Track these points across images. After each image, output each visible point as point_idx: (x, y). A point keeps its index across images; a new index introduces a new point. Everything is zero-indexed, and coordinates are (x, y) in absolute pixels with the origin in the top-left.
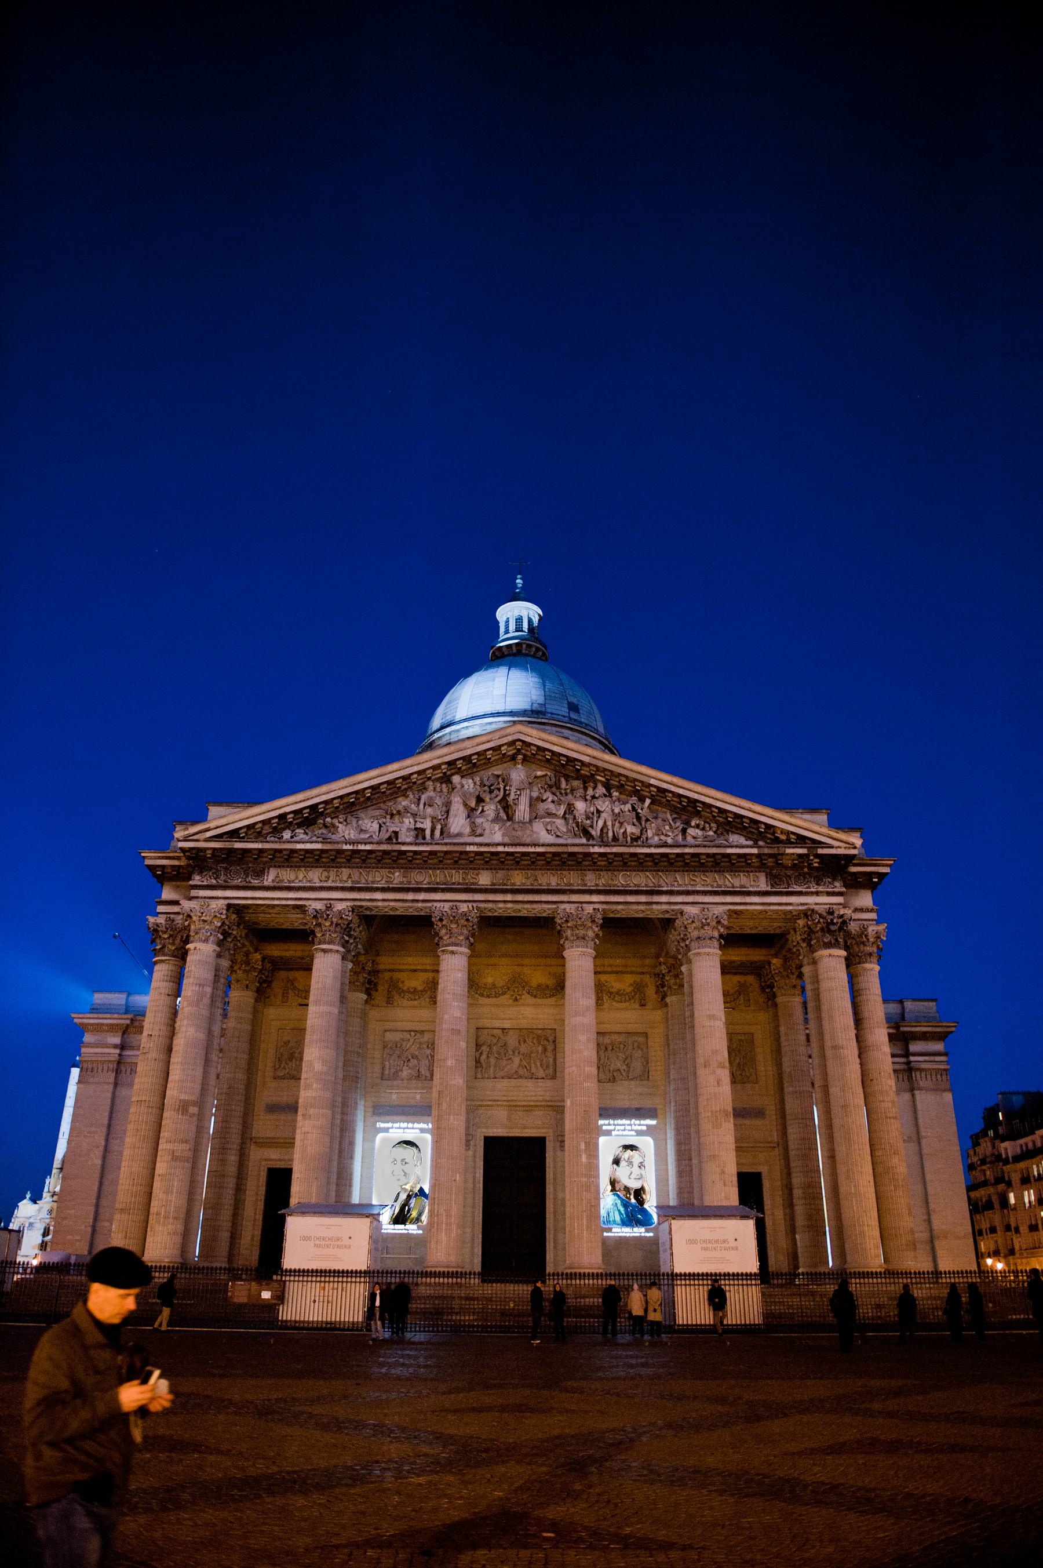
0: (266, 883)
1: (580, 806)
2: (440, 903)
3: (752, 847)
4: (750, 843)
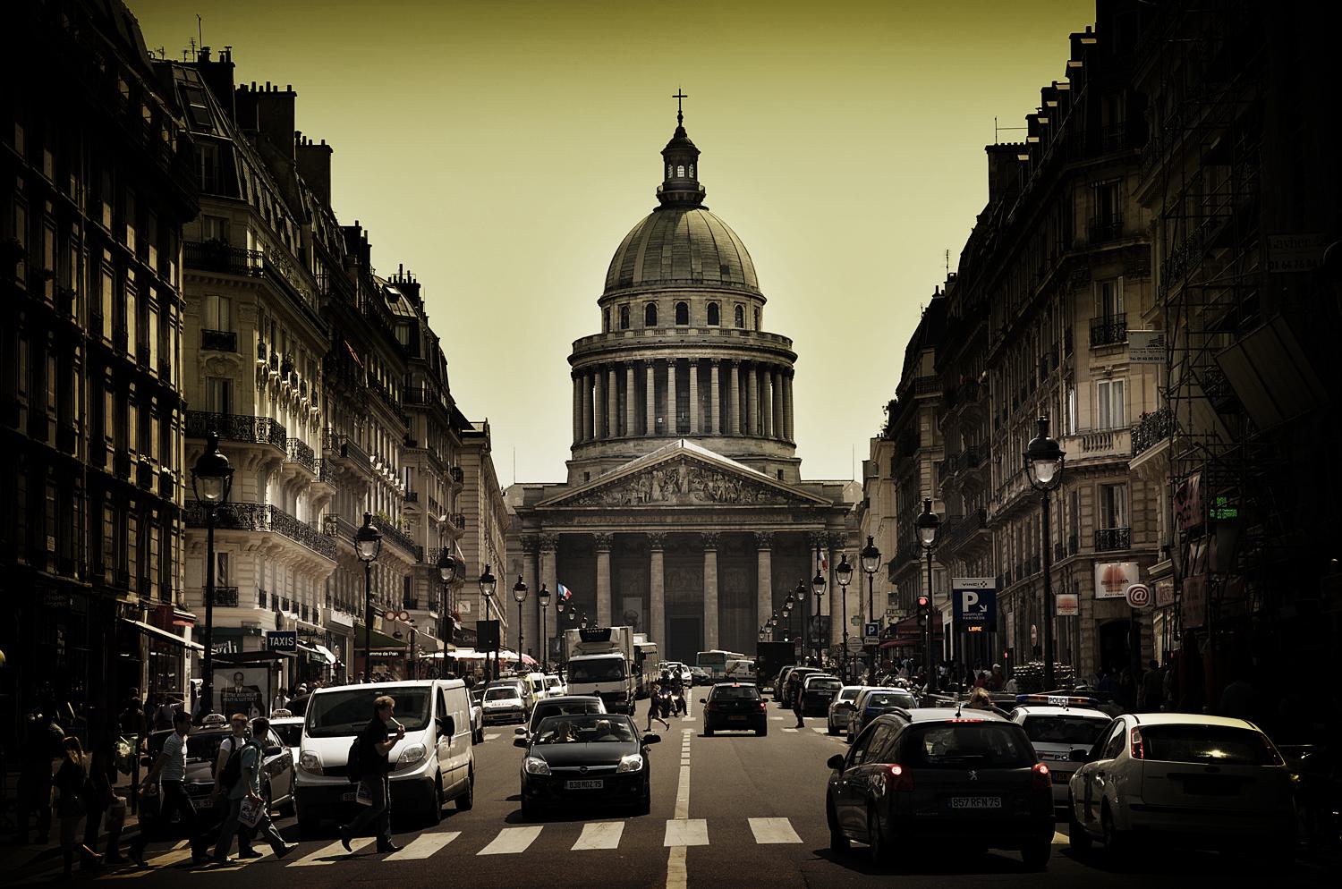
0: (575, 524)
1: (711, 484)
2: (650, 530)
3: (784, 504)
4: (785, 501)
